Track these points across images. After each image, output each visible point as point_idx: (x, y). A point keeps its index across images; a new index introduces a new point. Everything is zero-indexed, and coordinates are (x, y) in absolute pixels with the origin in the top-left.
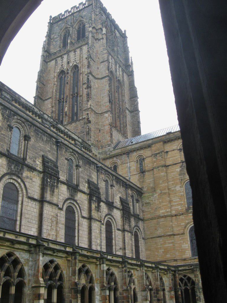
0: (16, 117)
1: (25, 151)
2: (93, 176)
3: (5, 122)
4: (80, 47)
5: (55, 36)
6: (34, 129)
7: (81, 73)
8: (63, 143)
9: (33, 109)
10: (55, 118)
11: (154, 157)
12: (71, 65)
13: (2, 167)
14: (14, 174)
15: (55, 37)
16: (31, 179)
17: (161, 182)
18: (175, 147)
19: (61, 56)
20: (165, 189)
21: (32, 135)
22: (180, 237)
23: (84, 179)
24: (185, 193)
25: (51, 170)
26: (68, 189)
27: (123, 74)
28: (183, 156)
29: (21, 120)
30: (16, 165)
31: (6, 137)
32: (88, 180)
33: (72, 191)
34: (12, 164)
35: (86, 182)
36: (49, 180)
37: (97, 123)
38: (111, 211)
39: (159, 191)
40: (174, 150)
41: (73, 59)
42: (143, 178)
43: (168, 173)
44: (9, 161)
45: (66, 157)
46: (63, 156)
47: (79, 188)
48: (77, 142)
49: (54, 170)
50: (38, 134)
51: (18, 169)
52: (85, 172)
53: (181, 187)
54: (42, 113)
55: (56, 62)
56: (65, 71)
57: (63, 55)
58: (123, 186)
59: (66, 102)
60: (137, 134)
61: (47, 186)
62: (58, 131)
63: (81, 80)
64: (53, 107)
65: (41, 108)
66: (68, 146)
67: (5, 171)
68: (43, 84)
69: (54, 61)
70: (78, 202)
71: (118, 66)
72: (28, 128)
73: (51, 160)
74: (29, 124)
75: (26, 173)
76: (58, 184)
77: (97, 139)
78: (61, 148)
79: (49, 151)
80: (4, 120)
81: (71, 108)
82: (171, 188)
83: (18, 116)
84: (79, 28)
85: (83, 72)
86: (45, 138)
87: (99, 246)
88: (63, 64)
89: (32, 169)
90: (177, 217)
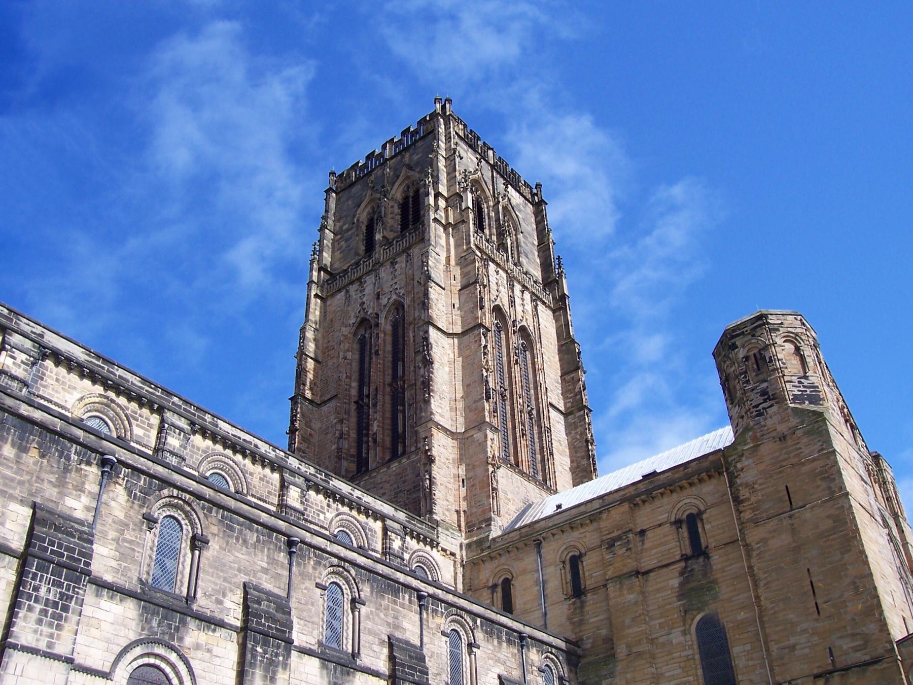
0: (166, 492)
1: (194, 577)
2: (405, 624)
3: (136, 507)
4: (406, 251)
5: (344, 224)
6: (220, 517)
7: (410, 324)
8: (310, 545)
9: (256, 446)
10: (349, 451)
11: (607, 548)
12: (384, 301)
13: (125, 626)
14: (158, 642)
15: (345, 227)
16: (209, 651)
17: (627, 621)
19: (359, 279)
20: (639, 642)
21: (213, 534)
23: (375, 635)
24: (697, 651)
25: (267, 619)
26: (324, 667)
27: (536, 310)
28: (687, 542)
29: (181, 499)
30: (165, 617)
31: (138, 547)
32: (389, 638)
33: (335, 672)
34: (153, 615)
36: (261, 648)
40: (660, 525)
41: (389, 284)
42: (582, 612)
43: (647, 594)
44: (144, 607)
45: (318, 581)
47: (358, 662)
48: (389, 522)
49: (275, 621)
50: (231, 529)
51: (169, 626)
52: (378, 615)
53: (684, 633)
54: (282, 454)
55: (348, 297)
56: (370, 319)
57: (363, 276)
58: (510, 642)
59: (375, 405)
60: (585, 477)
61: (253, 665)
62: (331, 500)
63: (412, 341)
64: (341, 421)
65: (311, 428)
66: (324, 551)
67: (133, 637)
69: (343, 293)
71: (518, 288)
72: (201, 516)
73: (268, 593)
74: (204, 505)
75: (194, 635)
76: (288, 655)
78: (302, 557)
79: (265, 571)
80: (133, 503)
81: (388, 421)
82: (657, 638)
83: (171, 489)
84: (406, 198)
85: (414, 319)
86: (252, 537)
88: (364, 300)
89: (212, 623)
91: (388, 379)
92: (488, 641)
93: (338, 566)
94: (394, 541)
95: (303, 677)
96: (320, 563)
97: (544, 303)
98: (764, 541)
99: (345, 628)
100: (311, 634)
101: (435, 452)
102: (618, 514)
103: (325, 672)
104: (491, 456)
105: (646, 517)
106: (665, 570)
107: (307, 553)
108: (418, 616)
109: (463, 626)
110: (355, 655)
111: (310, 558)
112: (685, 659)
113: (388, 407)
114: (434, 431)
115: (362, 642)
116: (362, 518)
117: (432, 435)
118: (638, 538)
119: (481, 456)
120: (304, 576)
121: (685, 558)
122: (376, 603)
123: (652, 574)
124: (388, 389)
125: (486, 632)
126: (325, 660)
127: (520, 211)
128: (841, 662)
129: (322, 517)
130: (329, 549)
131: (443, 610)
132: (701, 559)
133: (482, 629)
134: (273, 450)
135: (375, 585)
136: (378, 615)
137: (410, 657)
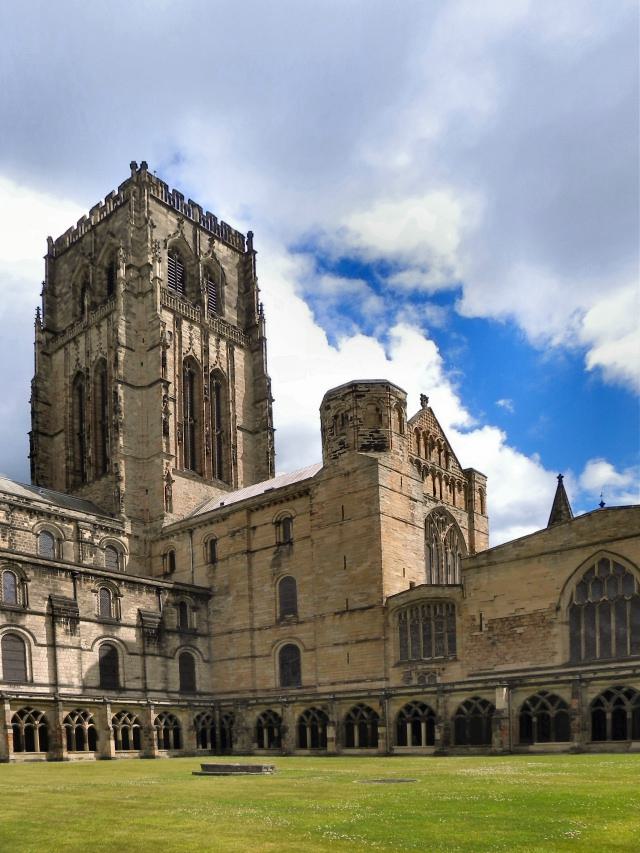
18: (268, 519)
37: (140, 477)
59: (89, 438)
68: (47, 404)
70: (27, 627)
91: (99, 418)
97: (241, 347)
102: (241, 516)
105: (257, 519)
106: (264, 552)
113: (99, 438)
118: (251, 531)
121: (279, 544)
124: (99, 426)
127: (226, 263)
129: (26, 525)
132: (288, 546)
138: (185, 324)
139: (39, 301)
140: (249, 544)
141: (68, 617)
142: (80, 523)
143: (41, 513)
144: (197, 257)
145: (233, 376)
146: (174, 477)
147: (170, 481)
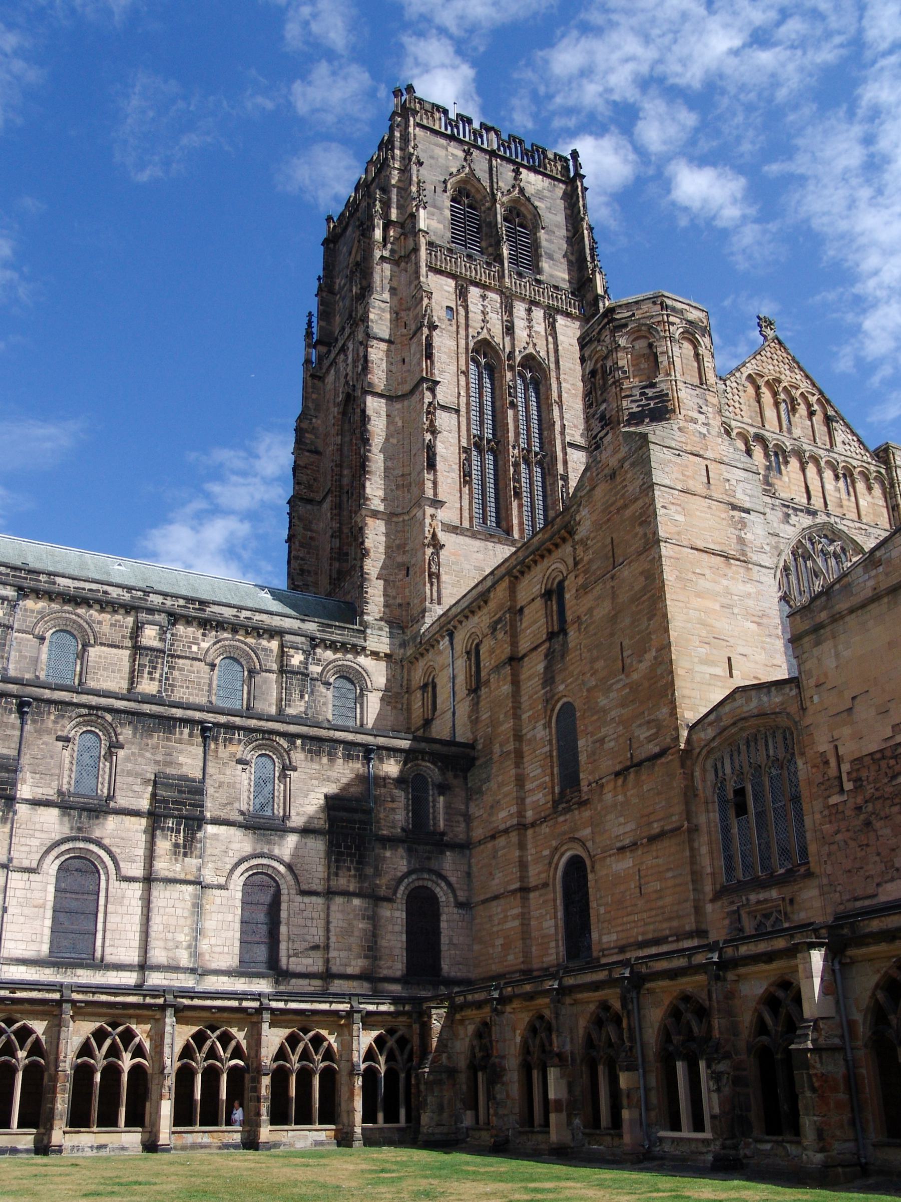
2: (182, 759)
8: (49, 702)
22: (541, 895)
23: (137, 775)
26: (63, 814)
35: (146, 782)
38: (269, 842)
39: (497, 749)
45: (59, 733)
46: (49, 733)
47: (112, 804)
58: (348, 757)
70: (106, 842)
77: (399, 601)
78: (40, 714)
87: (186, 949)
90: (537, 829)
92: (312, 760)
93: (90, 715)
94: (293, 656)
95: (38, 826)
96: (63, 716)
98: (590, 610)
99: (101, 772)
100: (49, 786)
101: (368, 544)
103: (66, 819)
104: (430, 536)
107: (46, 709)
108: (201, 749)
109: (275, 750)
110: (110, 797)
111: (49, 713)
112: (543, 756)
114: (369, 521)
115: (118, 784)
116: (250, 640)
117: (366, 524)
119: (422, 537)
120: (39, 732)
122: (140, 743)
123: (526, 659)
125: (310, 751)
126: (66, 808)
128: (642, 753)
130: (75, 700)
131: (242, 737)
133: (303, 749)
134: (127, 592)
135: (140, 726)
136: (143, 756)
137: (180, 792)
138: (474, 293)
139: (313, 305)
140: (514, 644)
141: (181, 817)
142: (288, 637)
143: (220, 625)
144: (494, 196)
145: (557, 362)
146: (442, 537)
147: (437, 546)
